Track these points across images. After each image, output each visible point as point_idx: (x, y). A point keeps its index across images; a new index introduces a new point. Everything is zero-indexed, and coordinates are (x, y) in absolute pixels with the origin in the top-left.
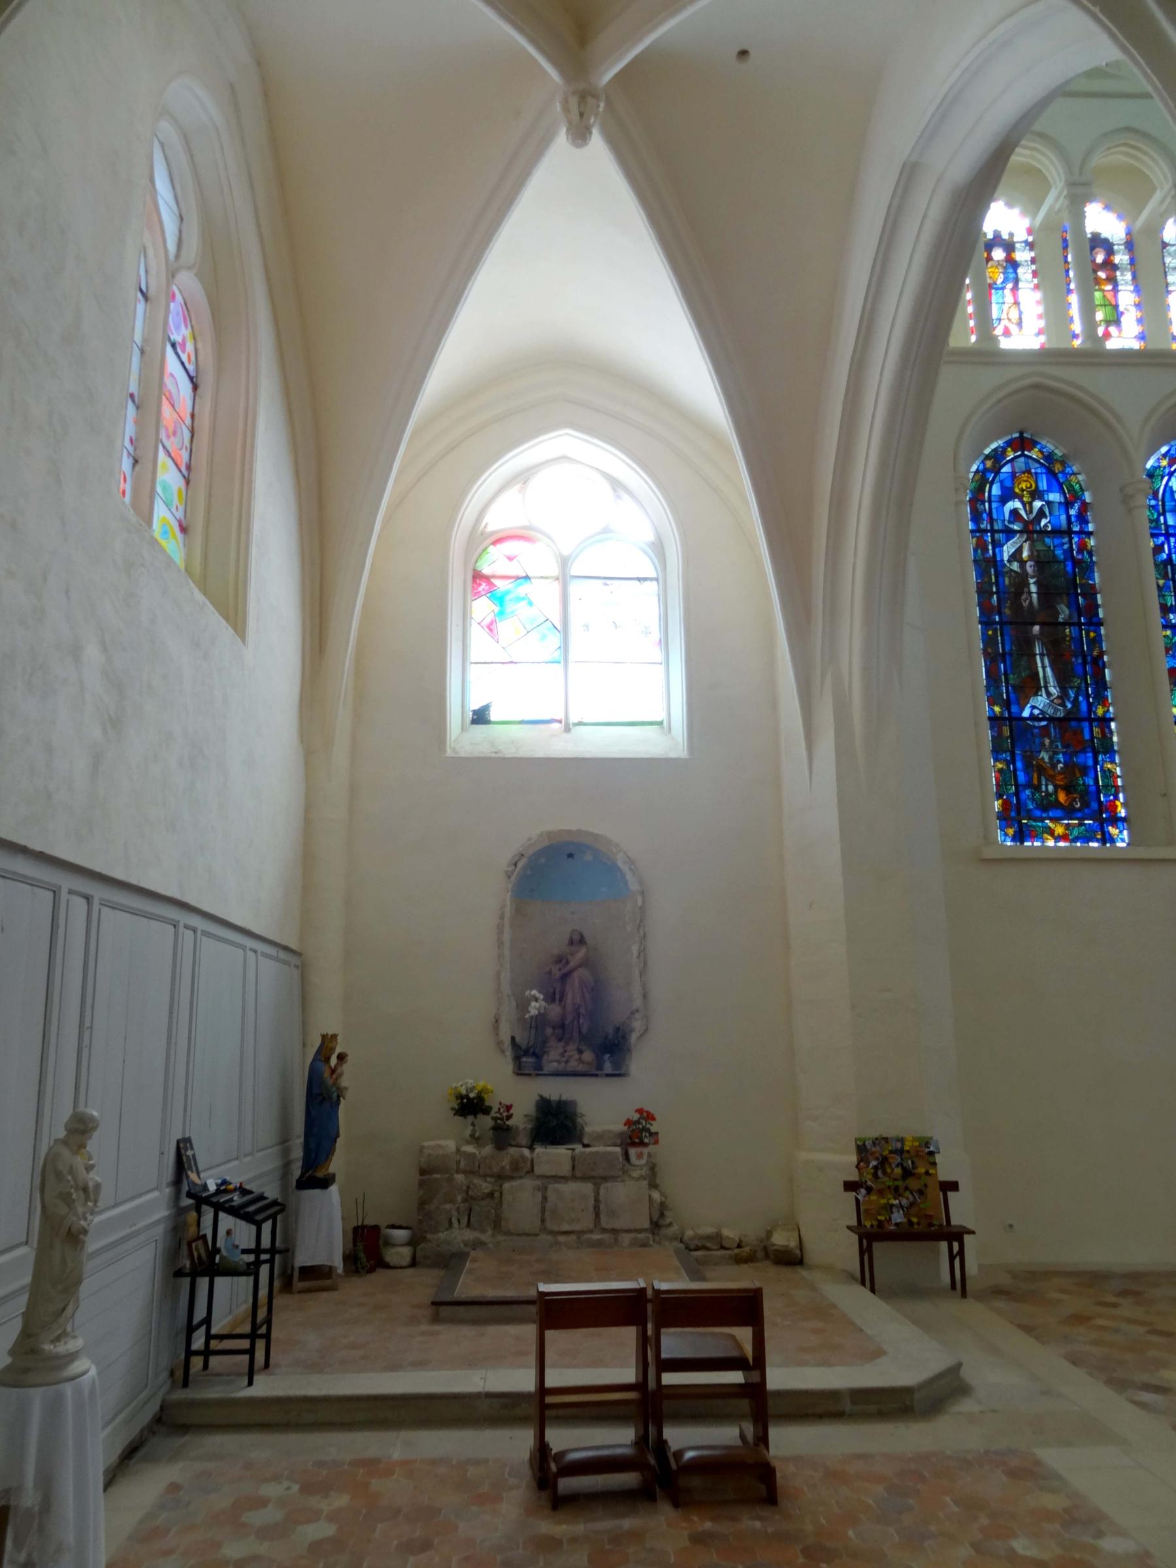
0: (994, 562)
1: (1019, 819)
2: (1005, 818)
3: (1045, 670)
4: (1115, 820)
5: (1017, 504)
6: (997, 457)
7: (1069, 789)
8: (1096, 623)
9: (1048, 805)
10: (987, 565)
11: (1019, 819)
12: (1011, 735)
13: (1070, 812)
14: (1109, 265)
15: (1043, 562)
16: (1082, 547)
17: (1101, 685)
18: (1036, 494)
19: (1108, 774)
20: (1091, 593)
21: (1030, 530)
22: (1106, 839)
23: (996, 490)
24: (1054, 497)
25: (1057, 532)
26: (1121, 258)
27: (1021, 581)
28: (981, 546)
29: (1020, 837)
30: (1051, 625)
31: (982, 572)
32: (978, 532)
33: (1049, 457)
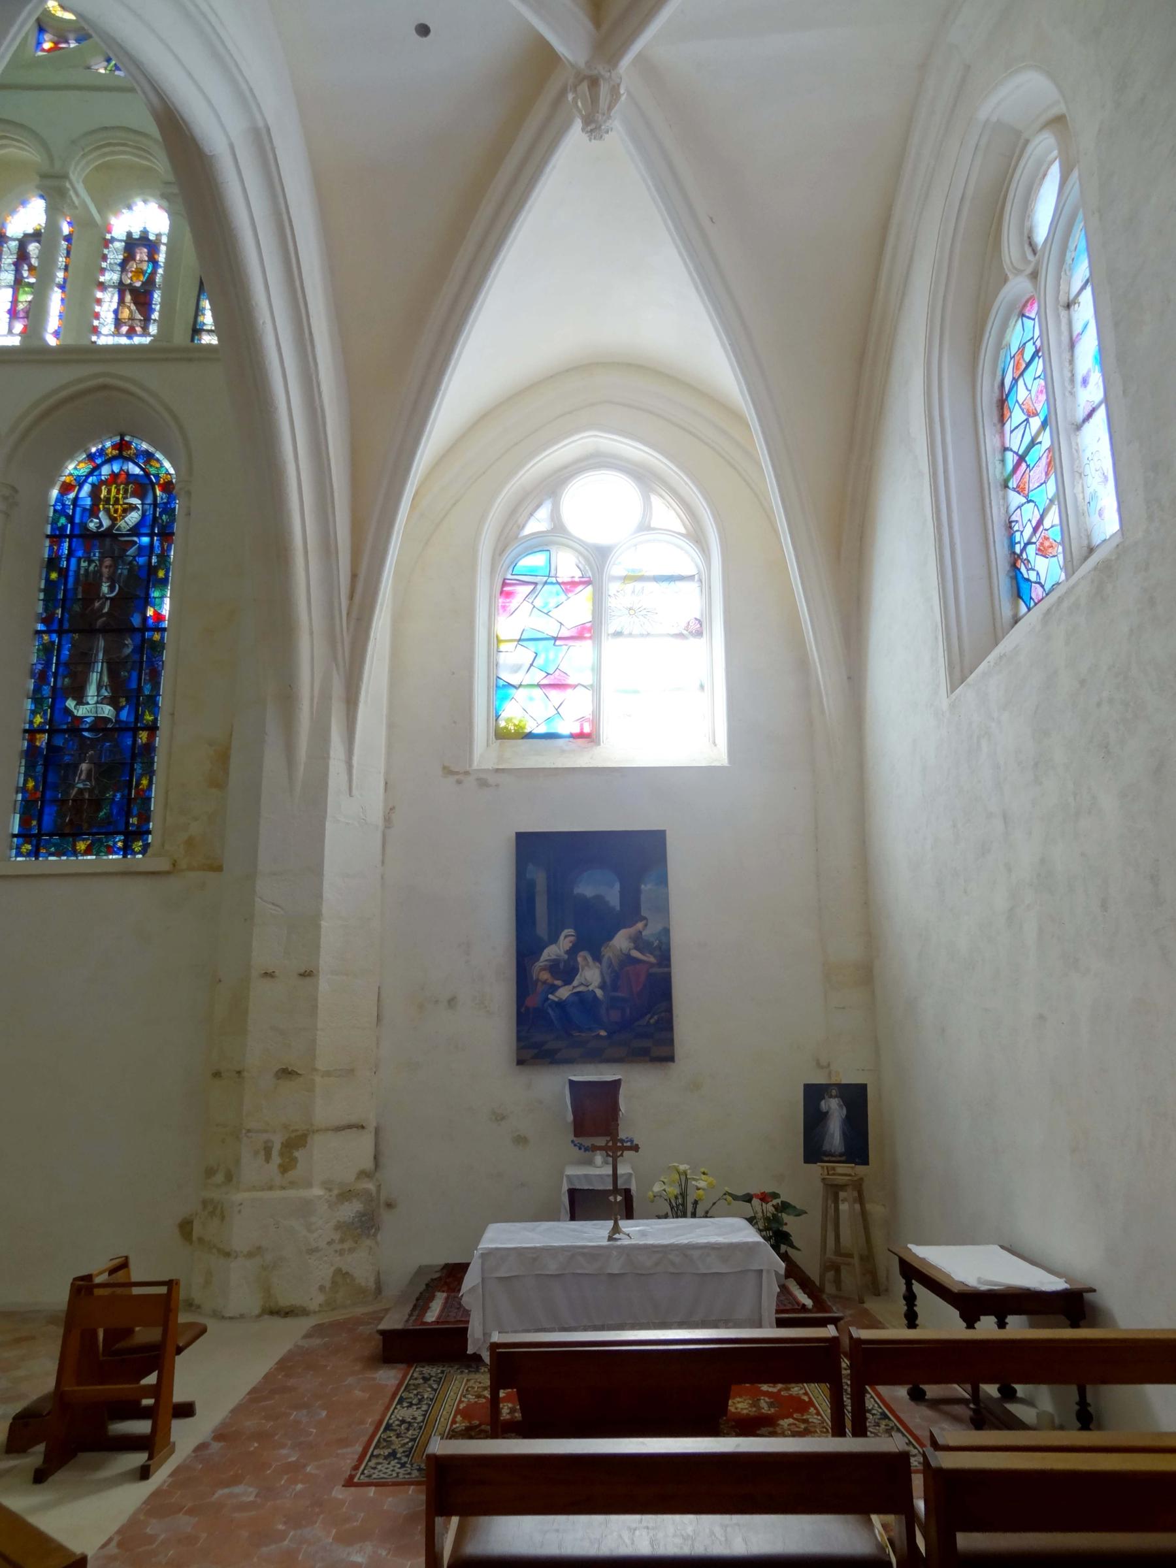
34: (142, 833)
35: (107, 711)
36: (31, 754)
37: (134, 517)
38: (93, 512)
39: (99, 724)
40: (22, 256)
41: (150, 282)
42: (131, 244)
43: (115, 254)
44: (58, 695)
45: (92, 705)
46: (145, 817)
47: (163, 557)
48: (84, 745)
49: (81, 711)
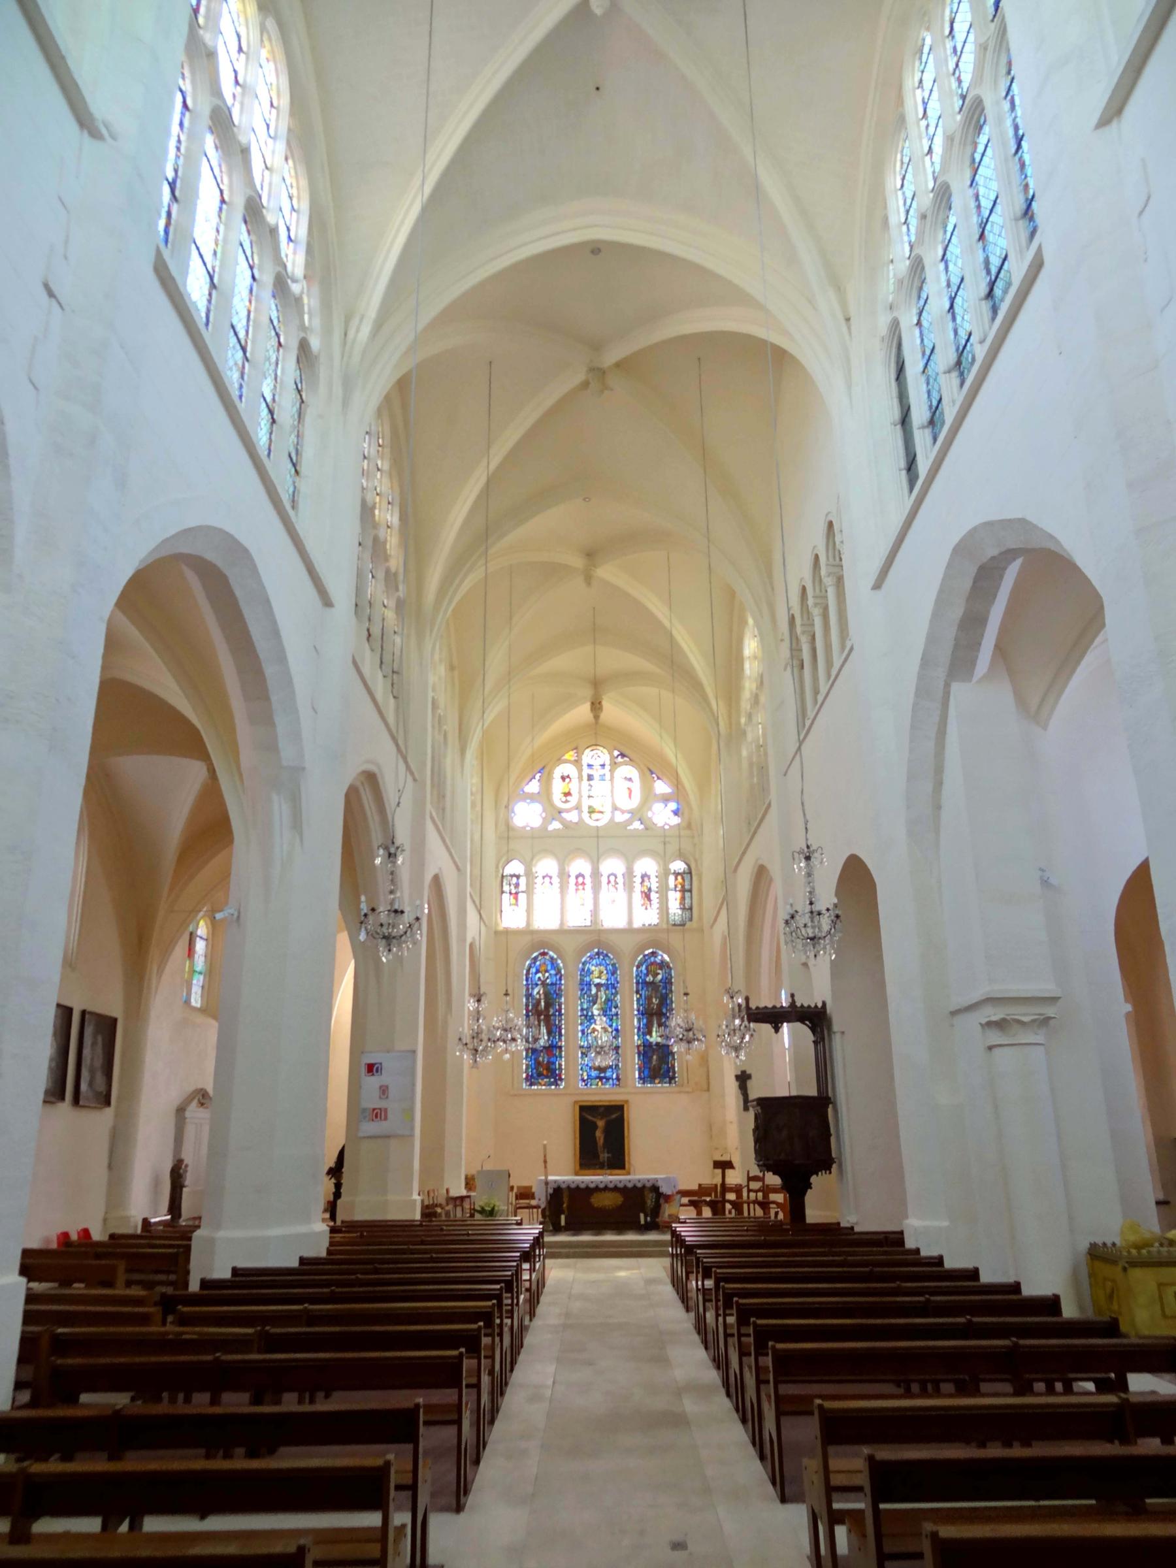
0: (531, 995)
1: (531, 1080)
2: (527, 1079)
3: (544, 1030)
4: (561, 1079)
5: (540, 975)
6: (535, 959)
7: (548, 1069)
8: (560, 1015)
9: (540, 1075)
10: (529, 996)
11: (531, 1080)
12: (533, 1052)
13: (547, 1077)
14: (583, 884)
15: (546, 994)
16: (560, 989)
17: (560, 1035)
18: (547, 971)
19: (560, 1065)
20: (560, 1006)
21: (544, 984)
22: (557, 1085)
23: (533, 970)
24: (553, 972)
25: (552, 984)
26: (588, 880)
27: (539, 1001)
28: (528, 989)
29: (531, 1085)
30: (548, 1017)
31: (527, 999)
32: (527, 985)
33: (552, 958)
34: (674, 1078)
35: (659, 1040)
36: (639, 1053)
37: (660, 977)
38: (647, 975)
39: (657, 1044)
40: (609, 882)
41: (650, 890)
42: (644, 876)
43: (638, 880)
44: (644, 1034)
45: (655, 1038)
46: (674, 1072)
47: (671, 991)
48: (654, 1051)
49: (651, 1040)
